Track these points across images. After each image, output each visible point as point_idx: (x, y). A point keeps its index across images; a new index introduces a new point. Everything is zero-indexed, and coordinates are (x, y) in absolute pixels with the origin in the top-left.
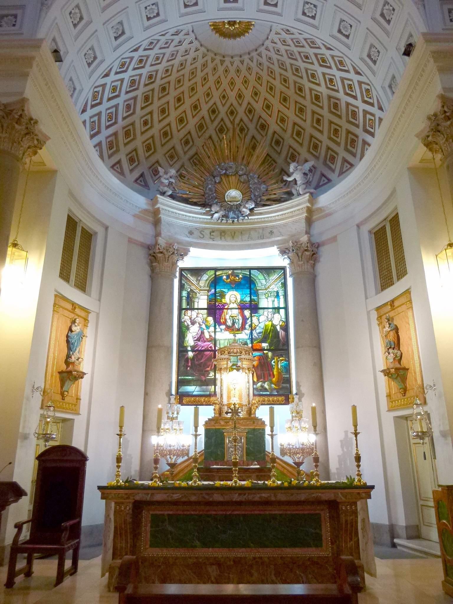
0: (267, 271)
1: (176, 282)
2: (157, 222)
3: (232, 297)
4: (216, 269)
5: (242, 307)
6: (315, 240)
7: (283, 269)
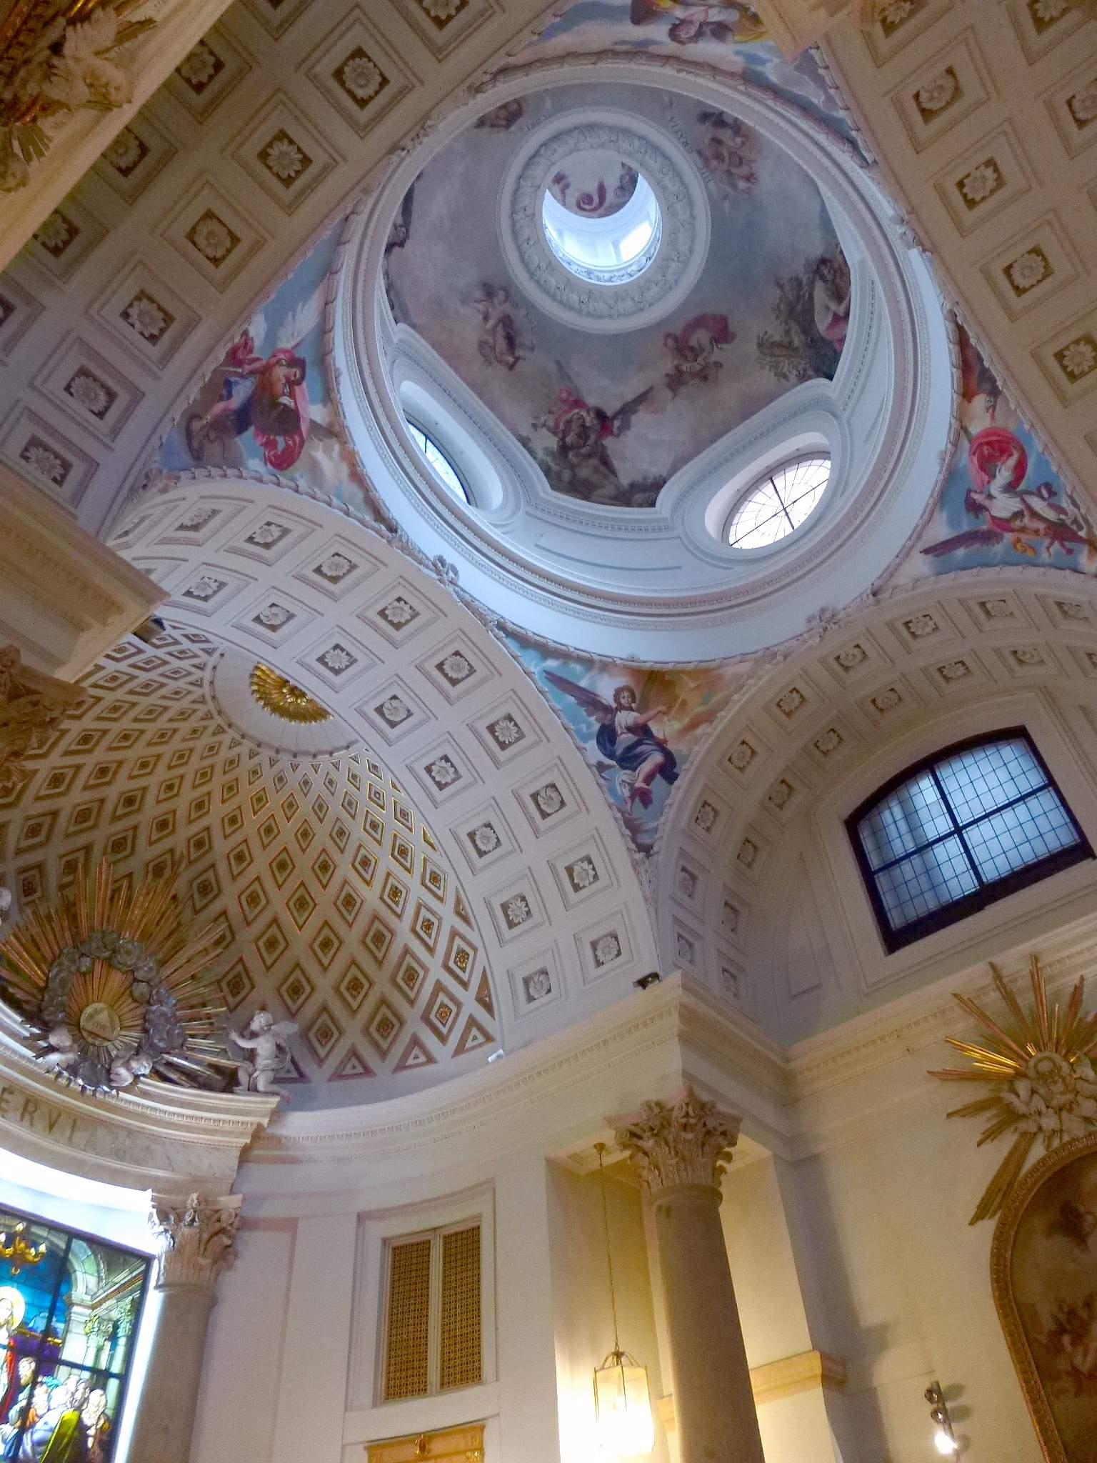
0: (113, 1255)
7: (147, 1260)
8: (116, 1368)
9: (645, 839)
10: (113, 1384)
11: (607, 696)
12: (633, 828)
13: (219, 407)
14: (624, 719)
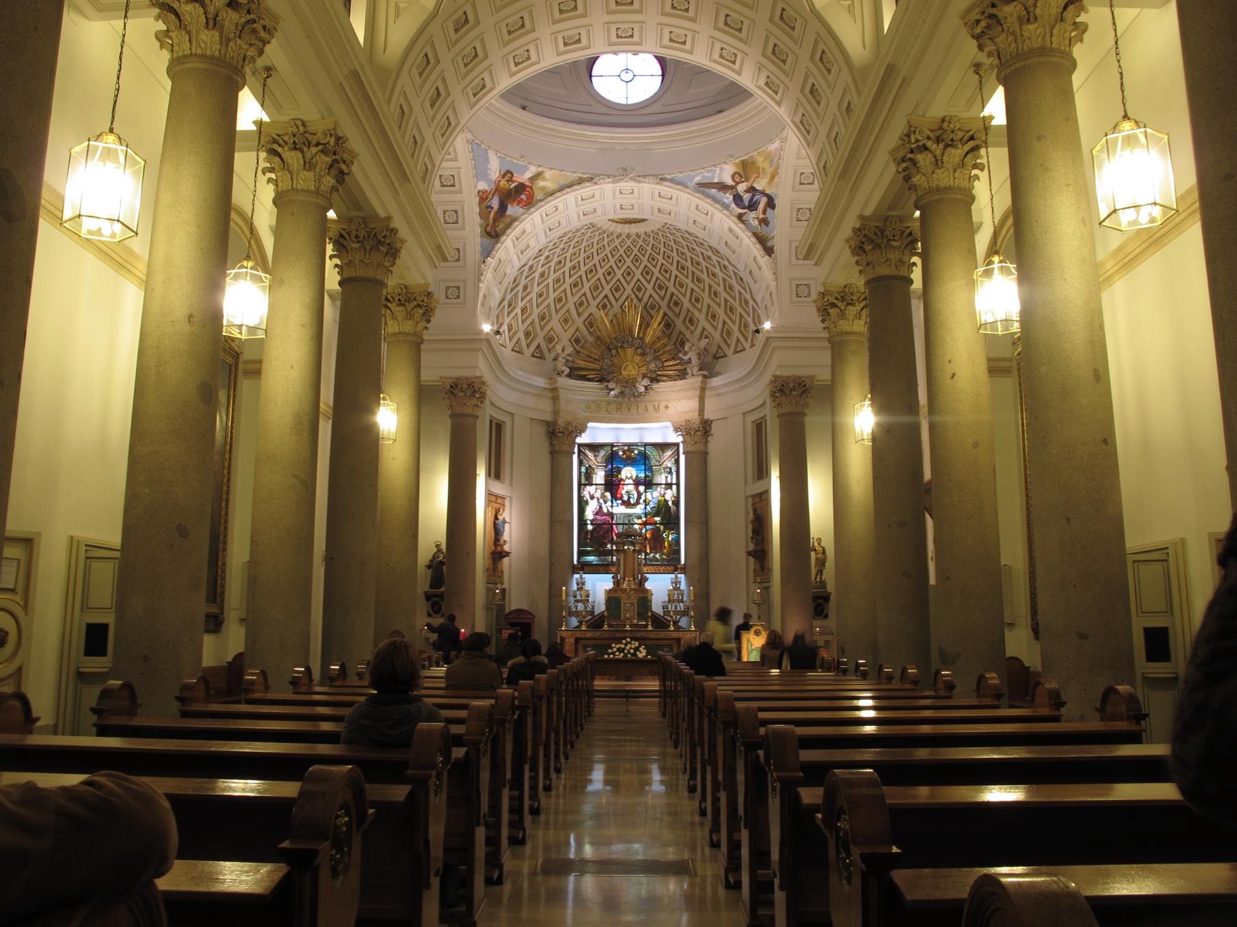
0: (662, 447)
1: (575, 457)
2: (555, 399)
3: (628, 473)
4: (612, 445)
5: (637, 483)
6: (706, 416)
7: (677, 445)
9: (769, 244)
10: (674, 487)
11: (729, 182)
12: (762, 240)
13: (492, 215)
14: (741, 188)
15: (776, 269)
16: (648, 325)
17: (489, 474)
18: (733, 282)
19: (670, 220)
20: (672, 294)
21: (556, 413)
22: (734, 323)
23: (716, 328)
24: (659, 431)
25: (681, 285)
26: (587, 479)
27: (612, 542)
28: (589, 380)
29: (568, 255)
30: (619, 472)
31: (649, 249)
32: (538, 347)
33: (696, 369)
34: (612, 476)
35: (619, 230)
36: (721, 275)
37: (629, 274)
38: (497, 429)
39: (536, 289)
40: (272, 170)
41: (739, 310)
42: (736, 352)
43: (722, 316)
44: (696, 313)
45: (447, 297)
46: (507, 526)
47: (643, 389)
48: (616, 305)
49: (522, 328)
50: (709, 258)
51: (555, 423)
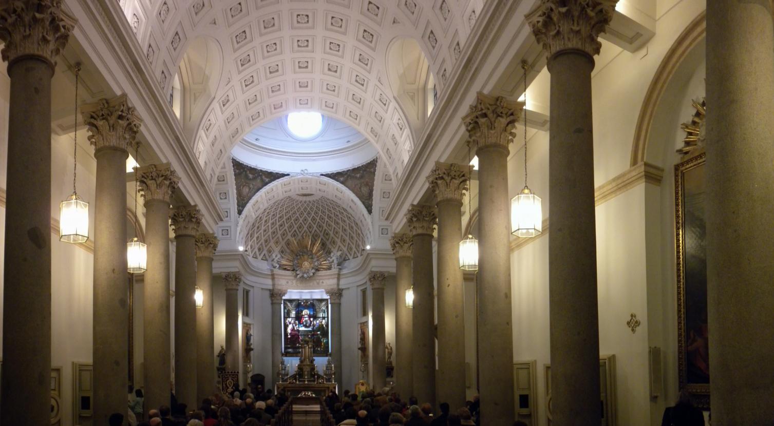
0: (321, 301)
1: (282, 305)
2: (273, 279)
3: (306, 312)
4: (298, 300)
5: (310, 317)
6: (340, 287)
7: (327, 300)
8: (326, 316)
10: (326, 319)
15: (373, 221)
16: (314, 244)
17: (243, 314)
18: (353, 225)
19: (324, 194)
20: (325, 230)
21: (274, 285)
22: (353, 244)
23: (345, 246)
24: (318, 294)
25: (329, 225)
26: (287, 315)
27: (299, 343)
28: (288, 270)
29: (278, 211)
30: (302, 312)
31: (315, 208)
32: (264, 255)
33: (336, 265)
34: (299, 314)
35: (301, 199)
36: (348, 221)
37: (305, 220)
38: (246, 293)
39: (263, 228)
40: (142, 190)
41: (356, 238)
42: (354, 258)
43: (348, 241)
44: (336, 239)
45: (223, 235)
46: (252, 337)
47: (312, 274)
48: (300, 235)
49: (257, 247)
50: (342, 213)
51: (273, 290)
